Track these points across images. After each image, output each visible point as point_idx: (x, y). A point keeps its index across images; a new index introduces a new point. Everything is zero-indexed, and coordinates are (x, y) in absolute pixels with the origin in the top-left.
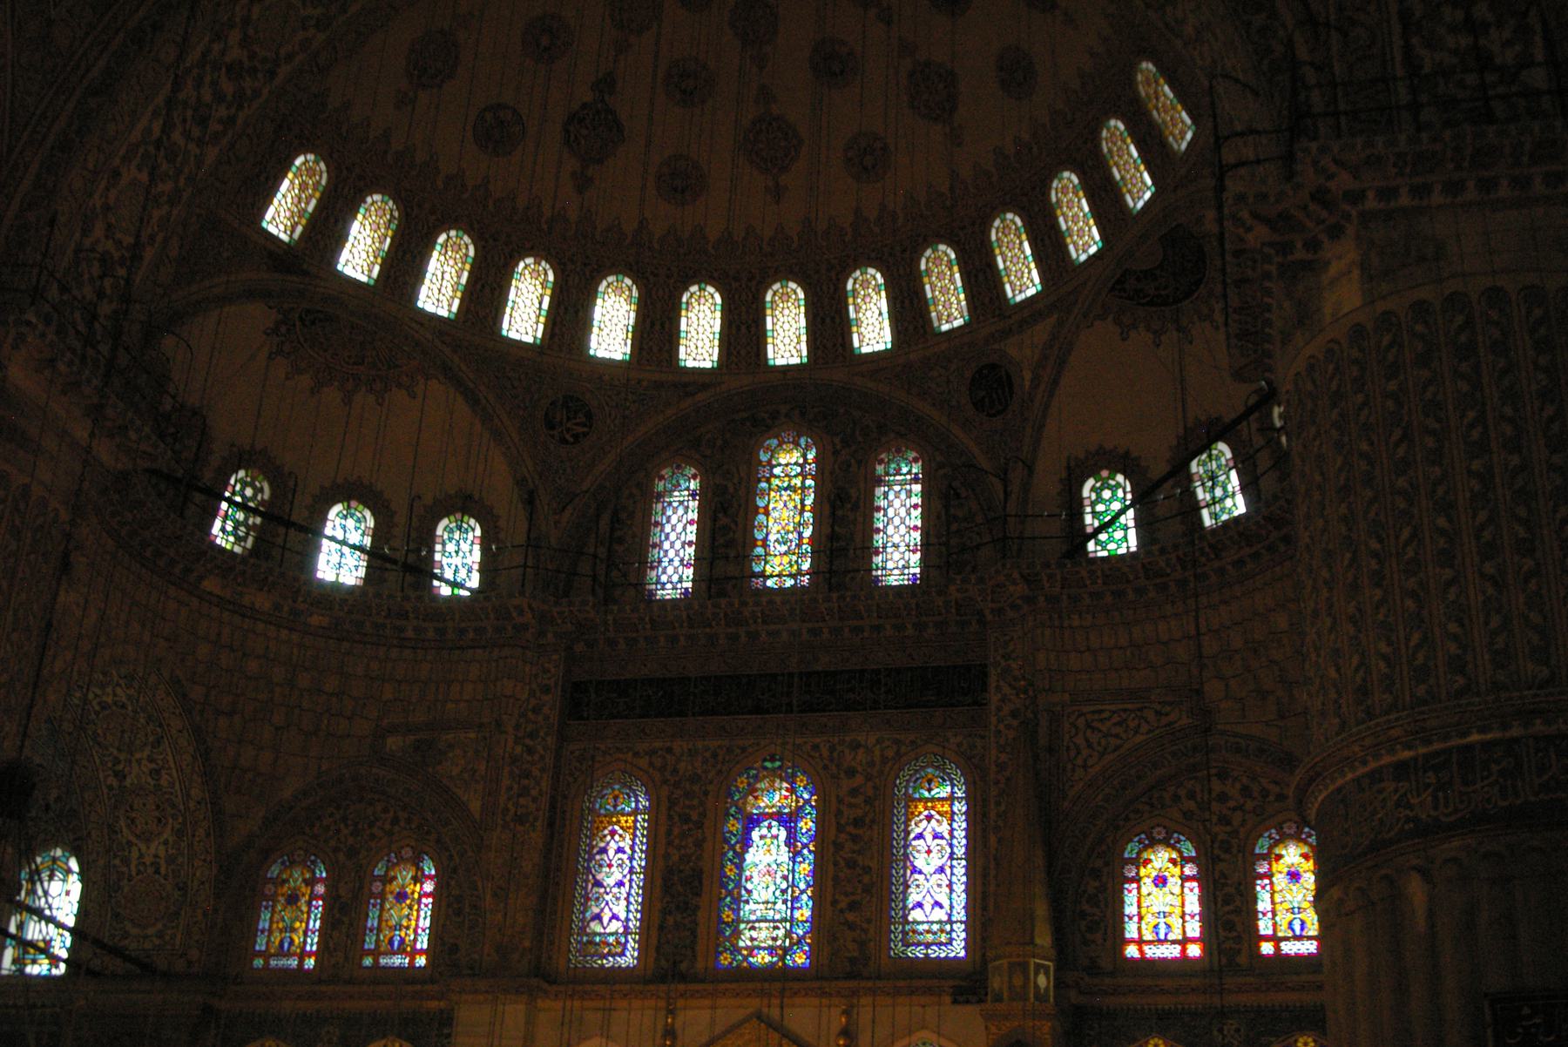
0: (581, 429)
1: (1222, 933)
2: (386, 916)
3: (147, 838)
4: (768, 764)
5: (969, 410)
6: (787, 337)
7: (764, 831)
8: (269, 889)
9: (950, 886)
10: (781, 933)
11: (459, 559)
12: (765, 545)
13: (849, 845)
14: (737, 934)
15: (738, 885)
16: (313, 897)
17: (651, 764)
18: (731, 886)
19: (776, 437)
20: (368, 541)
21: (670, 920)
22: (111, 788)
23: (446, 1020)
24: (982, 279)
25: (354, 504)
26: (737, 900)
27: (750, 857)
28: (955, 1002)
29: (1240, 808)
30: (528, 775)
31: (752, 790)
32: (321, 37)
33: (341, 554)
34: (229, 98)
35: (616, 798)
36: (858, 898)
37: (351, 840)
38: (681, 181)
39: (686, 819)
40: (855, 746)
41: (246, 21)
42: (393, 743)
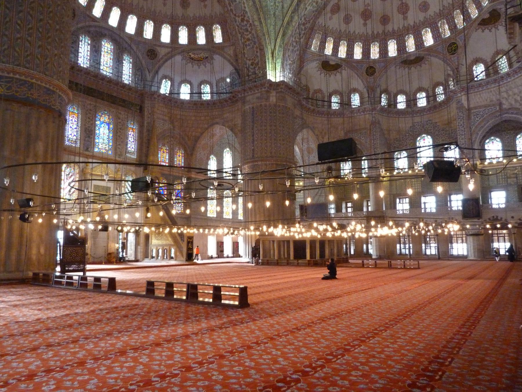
5: (150, 56)
10: (107, 147)
21: (86, 139)
24: (157, 32)
26: (99, 138)
39: (89, 118)
40: (120, 114)
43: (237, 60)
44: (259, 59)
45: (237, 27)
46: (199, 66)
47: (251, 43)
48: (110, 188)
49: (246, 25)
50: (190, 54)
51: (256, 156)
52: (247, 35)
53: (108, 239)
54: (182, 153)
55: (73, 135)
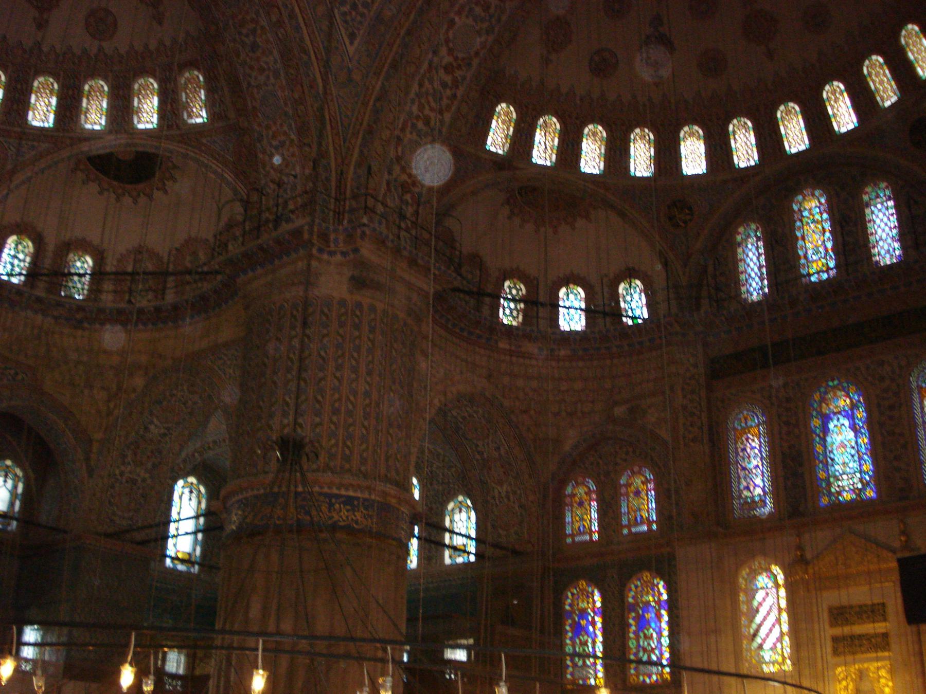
2: (630, 505)
3: (500, 483)
4: (831, 384)
6: (795, 136)
7: (835, 422)
8: (568, 500)
10: (855, 480)
11: (635, 303)
12: (806, 257)
14: (829, 484)
15: (825, 456)
16: (591, 500)
18: (821, 457)
20: (583, 306)
22: (477, 460)
23: (672, 557)
25: (571, 286)
27: (829, 439)
31: (823, 400)
32: (491, 38)
33: (572, 315)
34: (450, 84)
35: (746, 419)
39: (787, 423)
41: (447, 41)
42: (619, 411)
48: (883, 605)
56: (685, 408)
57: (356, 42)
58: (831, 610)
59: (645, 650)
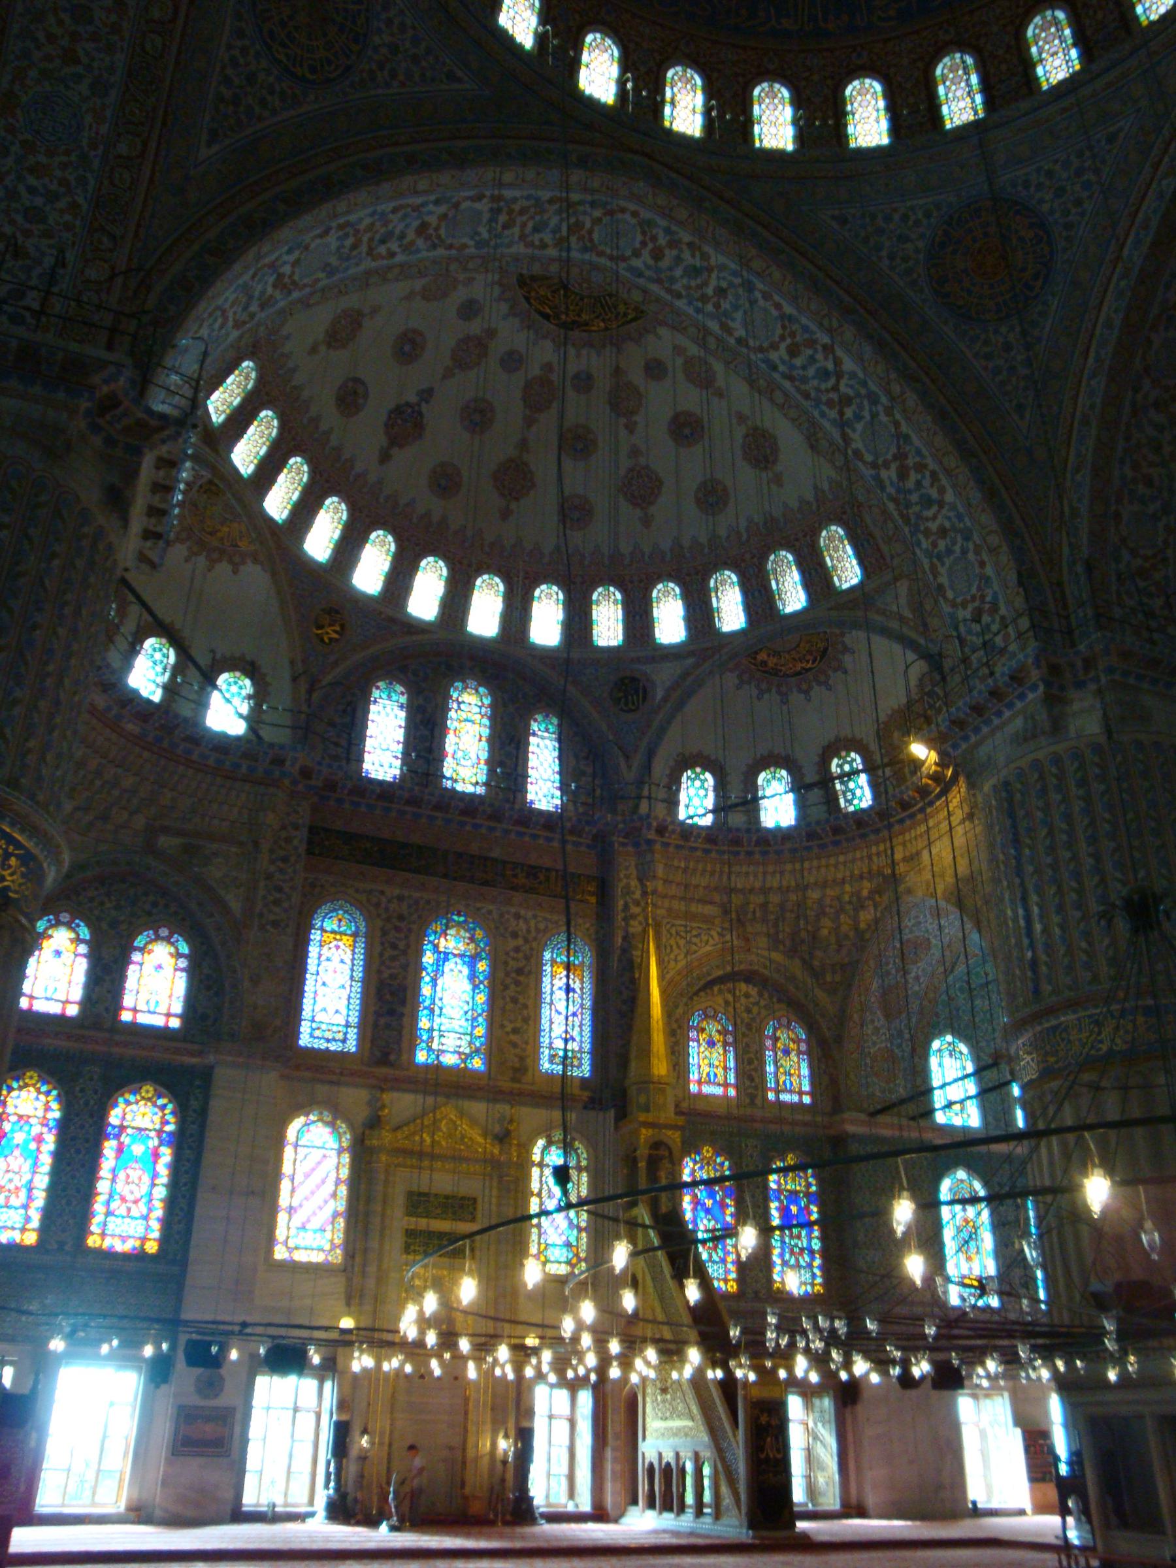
0: (335, 636)
1: (748, 1083)
6: (485, 614)
9: (581, 1026)
13: (513, 987)
14: (431, 1038)
17: (368, 901)
19: (463, 681)
21: (382, 1021)
23: (206, 1075)
24: (638, 619)
28: (585, 1108)
29: (757, 1004)
30: (279, 889)
31: (444, 934)
36: (518, 1025)
37: (114, 913)
38: (445, 481)
39: (394, 946)
40: (517, 916)
42: (165, 842)
43: (925, 625)
44: (996, 587)
45: (891, 506)
46: (806, 692)
47: (954, 543)
48: (475, 1200)
49: (919, 484)
50: (762, 656)
51: (1047, 988)
52: (934, 518)
53: (466, 1413)
54: (797, 1041)
55: (331, 1011)
56: (269, 877)
57: (216, 148)
58: (410, 1194)
59: (123, 1199)
